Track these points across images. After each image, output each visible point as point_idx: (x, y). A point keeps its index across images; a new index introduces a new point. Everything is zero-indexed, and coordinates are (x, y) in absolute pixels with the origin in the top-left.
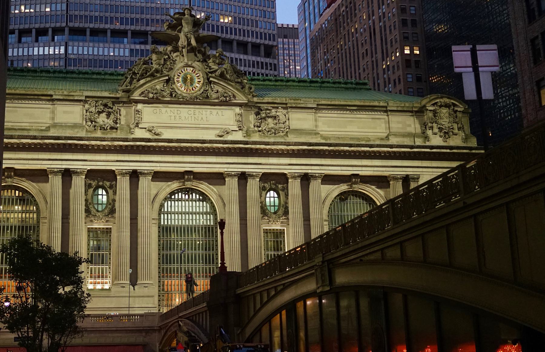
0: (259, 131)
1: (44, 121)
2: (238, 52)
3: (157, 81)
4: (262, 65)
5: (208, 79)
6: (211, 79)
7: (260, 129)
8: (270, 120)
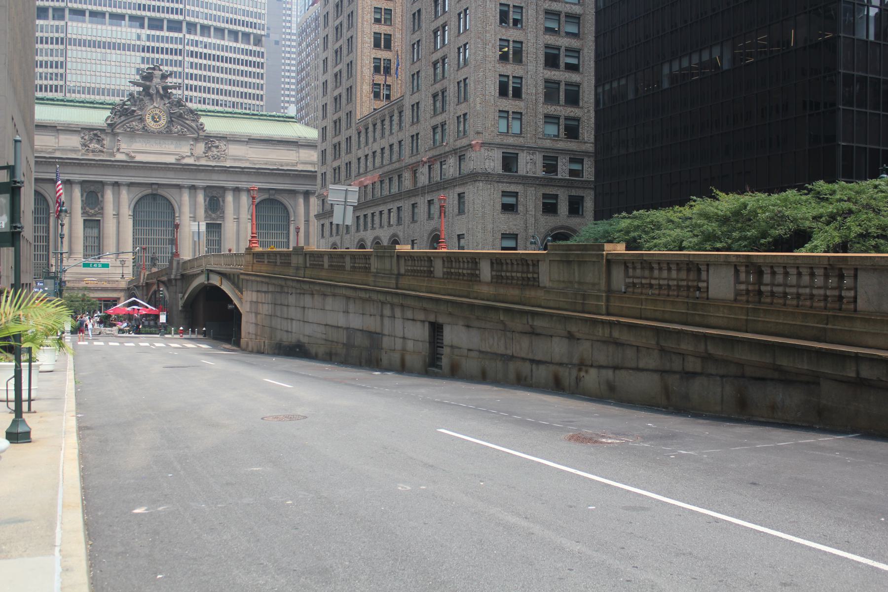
0: (206, 156)
1: (51, 144)
2: (229, 40)
3: (133, 119)
4: (250, 53)
5: (171, 118)
6: (173, 119)
7: (207, 155)
8: (214, 149)
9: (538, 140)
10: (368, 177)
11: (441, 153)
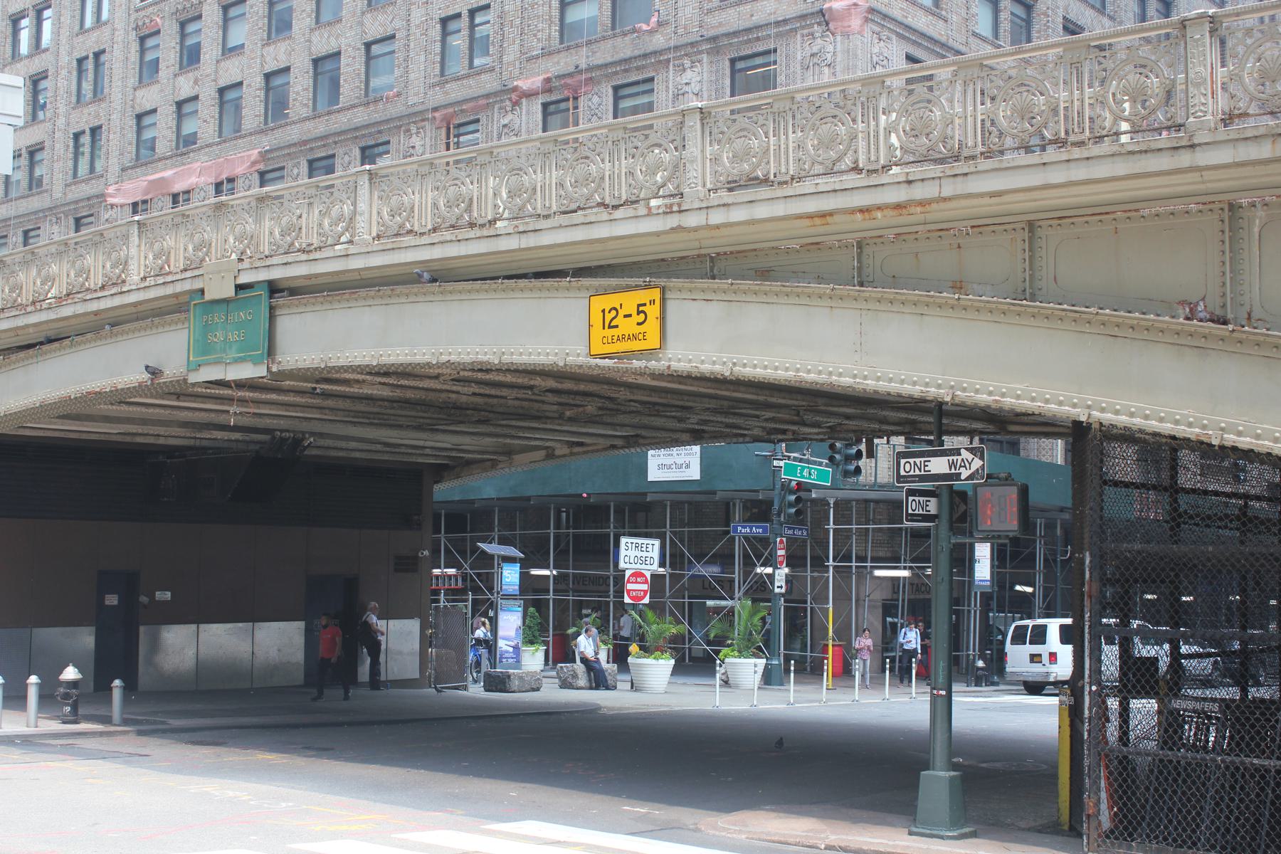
9: (971, 39)
10: (196, 165)
11: (621, 56)
